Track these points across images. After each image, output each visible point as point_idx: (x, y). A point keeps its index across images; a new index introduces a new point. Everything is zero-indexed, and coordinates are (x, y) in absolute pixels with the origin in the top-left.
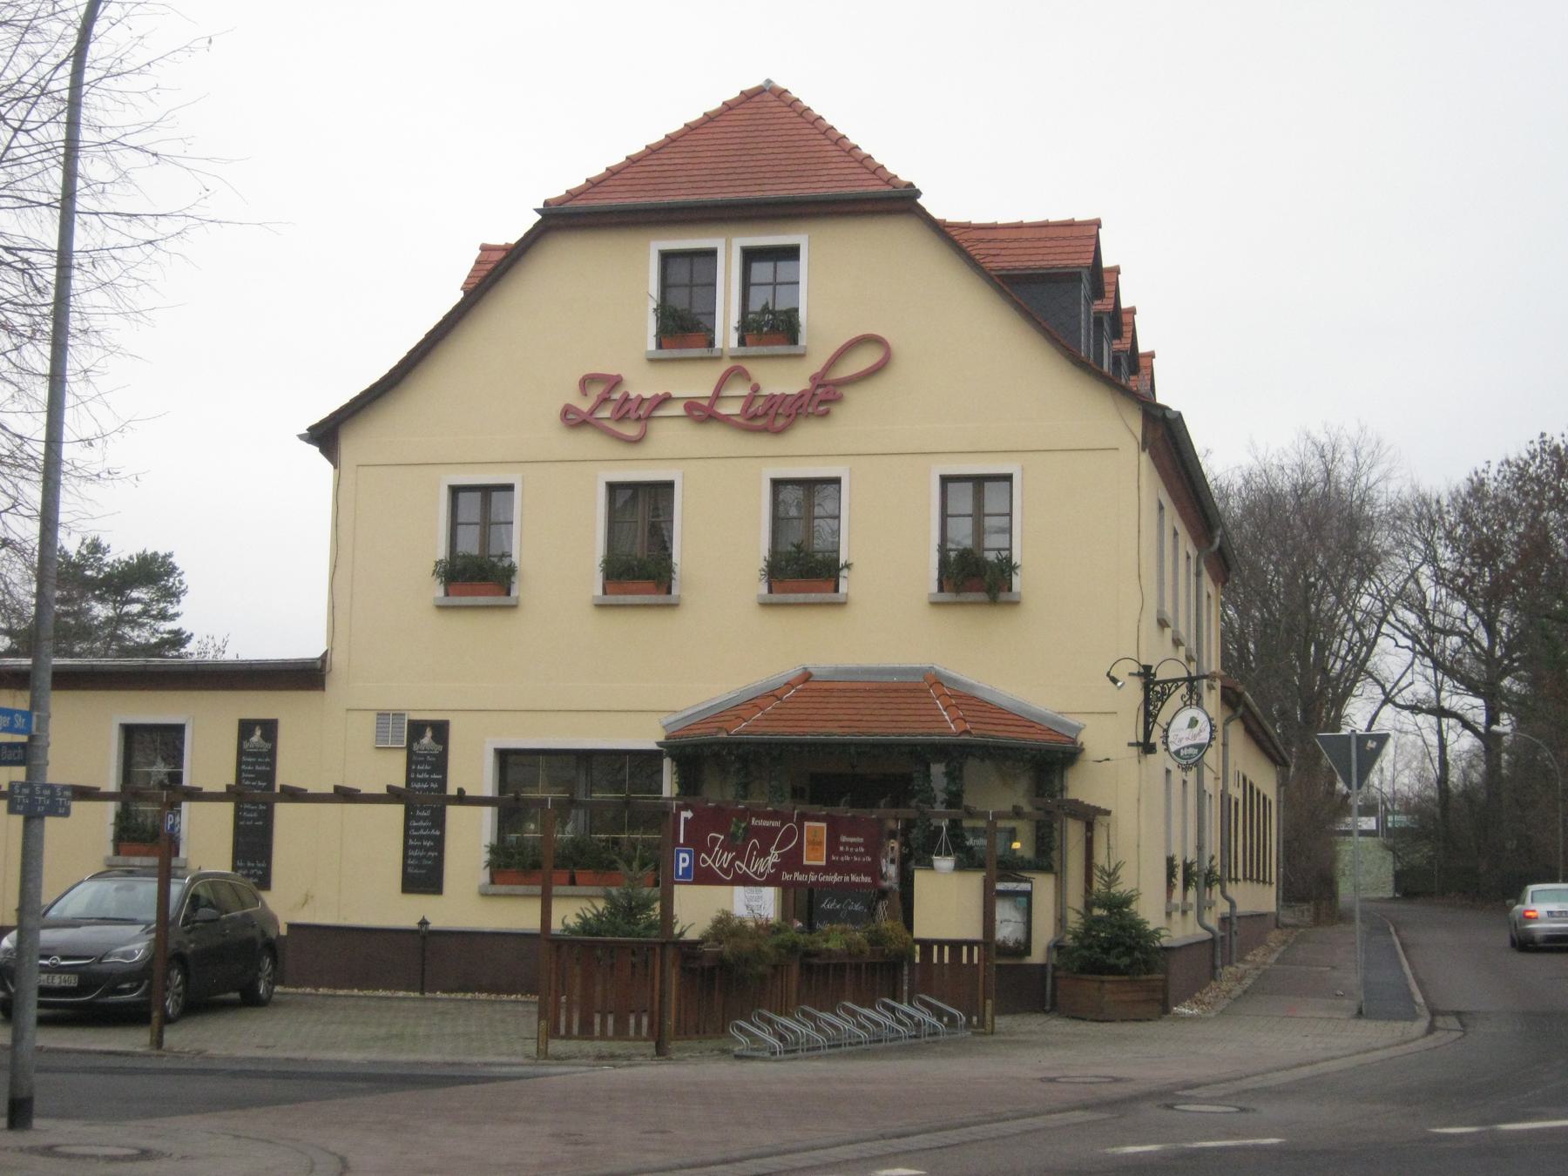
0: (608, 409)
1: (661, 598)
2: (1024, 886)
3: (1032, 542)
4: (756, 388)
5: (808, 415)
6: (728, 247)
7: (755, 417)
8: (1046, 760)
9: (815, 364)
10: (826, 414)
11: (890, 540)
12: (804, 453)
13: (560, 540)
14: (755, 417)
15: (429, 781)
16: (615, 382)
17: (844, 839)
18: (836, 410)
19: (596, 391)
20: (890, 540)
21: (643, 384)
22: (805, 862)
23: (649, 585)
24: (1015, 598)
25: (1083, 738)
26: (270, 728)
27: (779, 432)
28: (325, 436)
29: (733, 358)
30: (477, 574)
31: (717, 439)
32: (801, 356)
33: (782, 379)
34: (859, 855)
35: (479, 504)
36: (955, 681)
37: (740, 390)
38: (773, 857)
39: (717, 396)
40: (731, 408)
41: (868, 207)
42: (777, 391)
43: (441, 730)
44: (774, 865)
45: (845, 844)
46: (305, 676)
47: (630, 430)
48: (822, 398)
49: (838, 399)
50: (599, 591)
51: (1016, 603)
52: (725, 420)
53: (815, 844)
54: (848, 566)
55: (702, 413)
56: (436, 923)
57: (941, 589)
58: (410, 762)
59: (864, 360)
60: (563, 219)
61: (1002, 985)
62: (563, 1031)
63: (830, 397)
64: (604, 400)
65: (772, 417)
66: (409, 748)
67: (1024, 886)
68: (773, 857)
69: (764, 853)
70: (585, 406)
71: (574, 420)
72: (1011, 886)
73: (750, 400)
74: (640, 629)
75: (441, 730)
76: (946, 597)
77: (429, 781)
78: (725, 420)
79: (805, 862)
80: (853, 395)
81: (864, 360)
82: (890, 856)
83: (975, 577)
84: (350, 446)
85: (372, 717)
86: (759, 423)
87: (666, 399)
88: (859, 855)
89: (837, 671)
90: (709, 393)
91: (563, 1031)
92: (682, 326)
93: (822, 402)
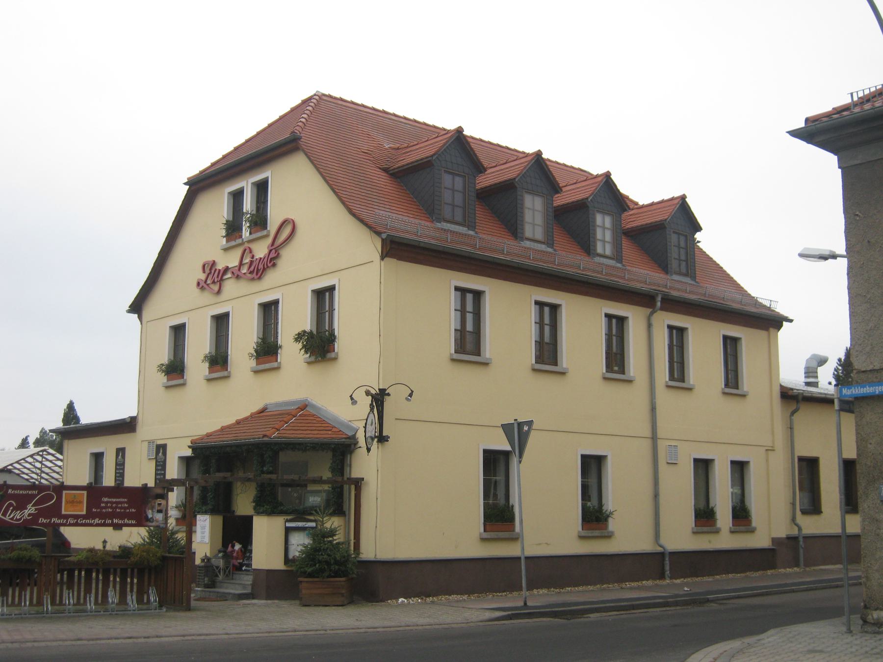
3: (346, 324)
10: (274, 265)
12: (269, 288)
17: (106, 499)
22: (63, 512)
28: (137, 307)
34: (121, 508)
37: (247, 260)
38: (31, 509)
40: (244, 270)
44: (29, 515)
45: (107, 503)
46: (127, 426)
47: (216, 288)
50: (207, 373)
53: (72, 502)
58: (156, 465)
60: (200, 185)
66: (156, 458)
68: (31, 509)
69: (21, 507)
72: (300, 524)
73: (251, 263)
79: (63, 512)
82: (157, 507)
83: (320, 345)
84: (146, 313)
87: (227, 269)
88: (125, 508)
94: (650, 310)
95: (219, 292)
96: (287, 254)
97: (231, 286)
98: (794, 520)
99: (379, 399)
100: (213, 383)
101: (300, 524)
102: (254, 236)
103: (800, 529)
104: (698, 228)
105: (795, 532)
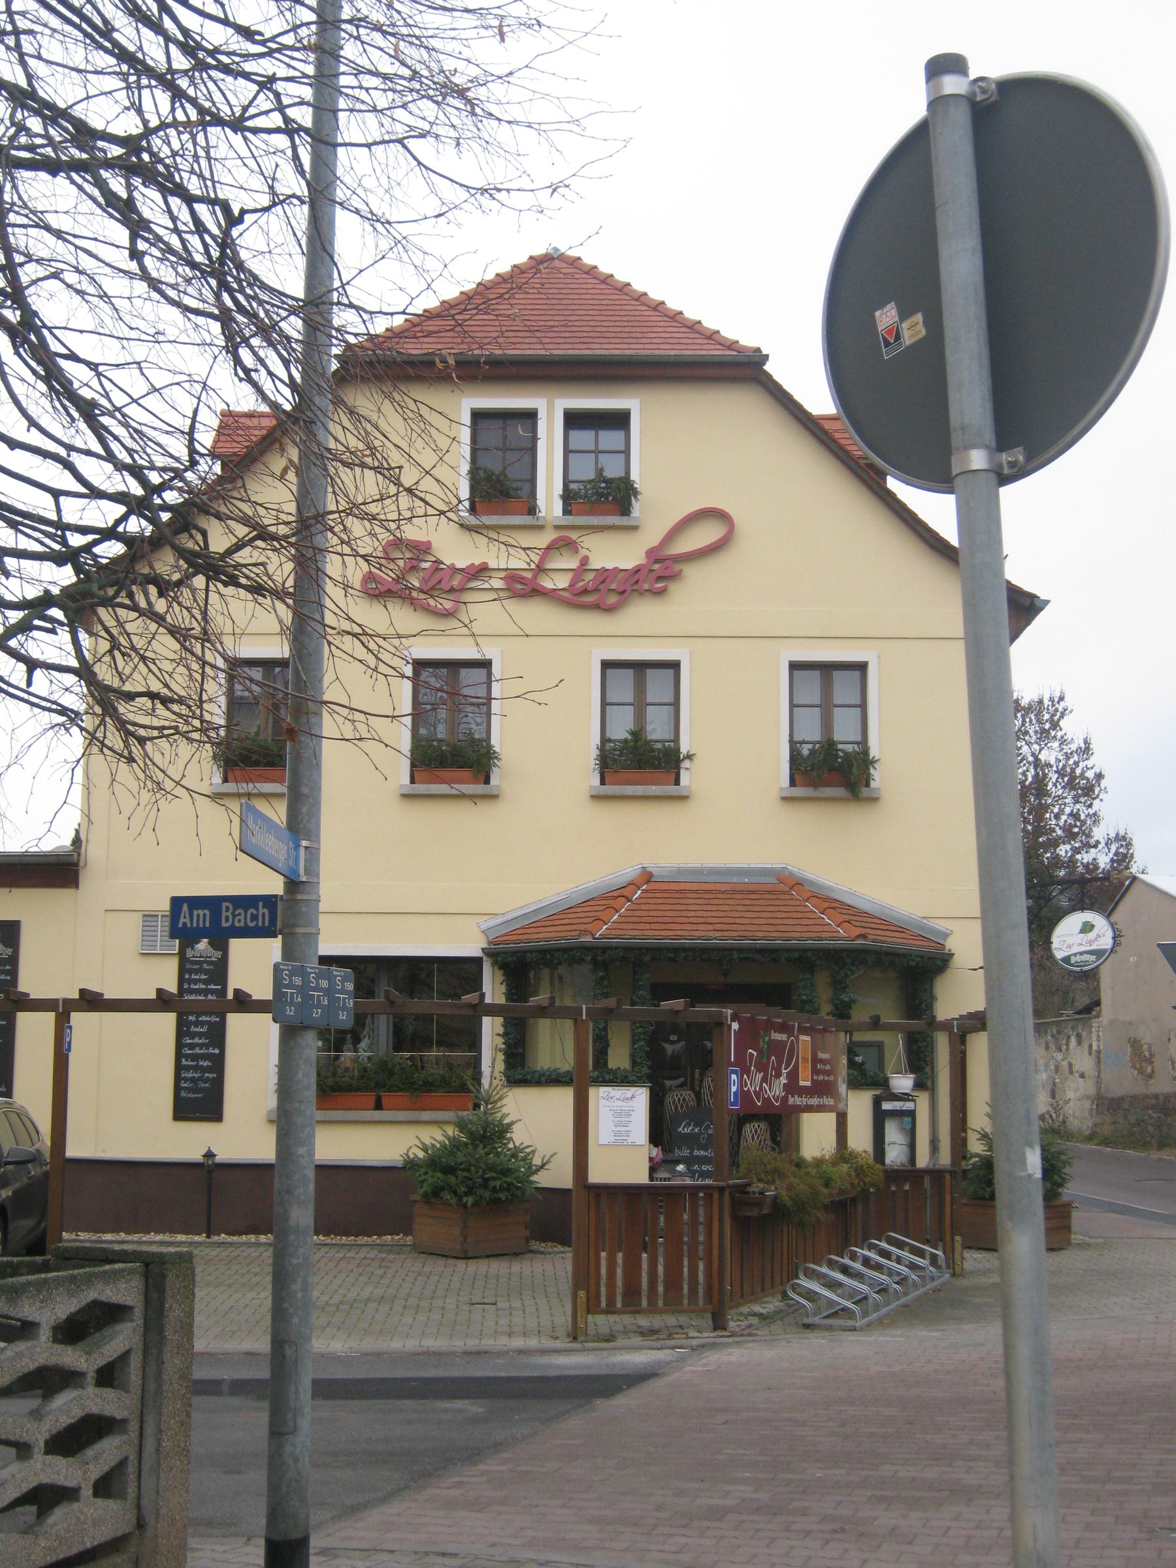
1: (479, 789)
4: (585, 561)
5: (642, 593)
6: (550, 408)
7: (585, 591)
8: (915, 968)
9: (651, 536)
10: (661, 593)
12: (639, 631)
14: (585, 591)
15: (205, 992)
18: (674, 587)
20: (737, 734)
23: (465, 773)
24: (874, 795)
25: (951, 944)
27: (610, 609)
29: (557, 527)
31: (537, 616)
33: (614, 553)
36: (812, 883)
39: (540, 569)
41: (710, 372)
42: (610, 566)
46: (56, 871)
48: (659, 574)
49: (674, 577)
50: (406, 780)
51: (876, 799)
52: (550, 595)
54: (689, 757)
55: (524, 587)
56: (223, 1155)
57: (793, 783)
58: (182, 970)
59: (704, 535)
62: (603, 1304)
63: (667, 573)
65: (599, 594)
74: (453, 822)
76: (799, 791)
77: (205, 992)
78: (550, 595)
80: (693, 573)
81: (704, 535)
85: (138, 917)
86: (589, 599)
87: (481, 571)
89: (680, 871)
91: (603, 1304)
92: (498, 489)
93: (660, 578)
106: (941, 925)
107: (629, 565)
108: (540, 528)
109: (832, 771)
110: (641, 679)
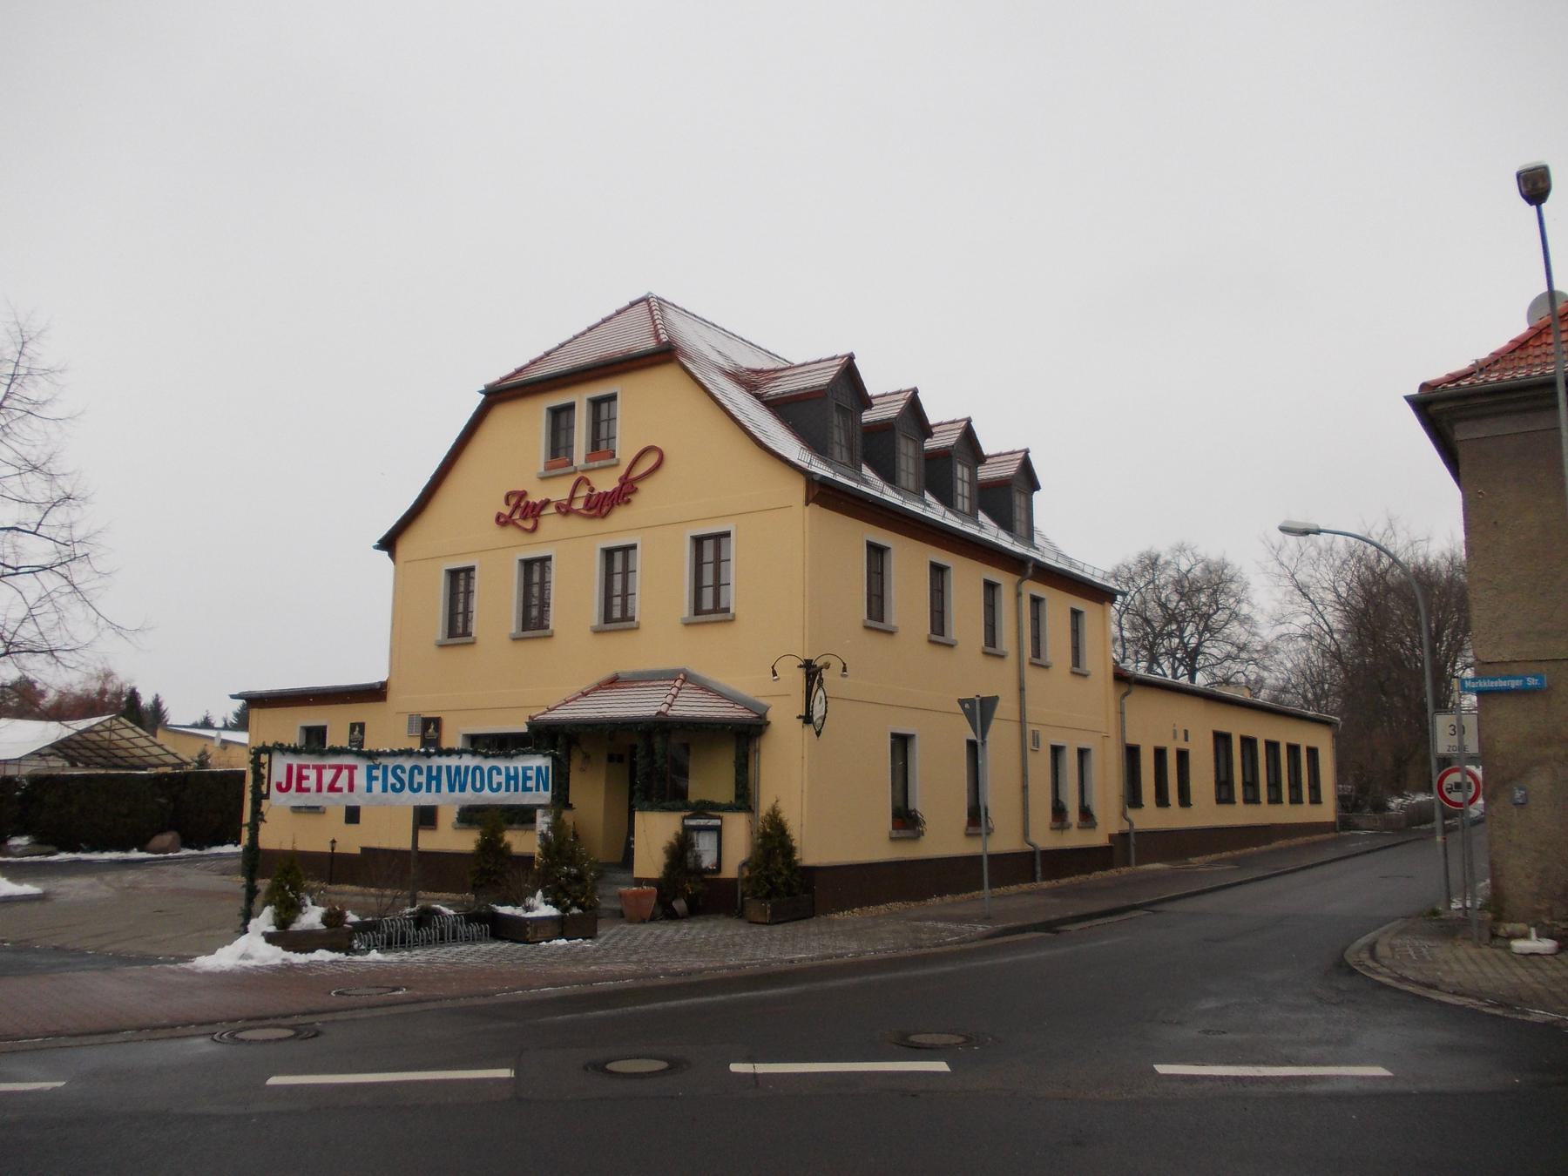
0: (523, 511)
2: (718, 822)
4: (592, 490)
6: (580, 398)
9: (622, 471)
10: (629, 501)
11: (662, 583)
12: (618, 528)
13: (497, 602)
16: (523, 494)
19: (513, 501)
20: (662, 583)
21: (535, 497)
26: (362, 726)
27: (604, 516)
28: (389, 543)
30: (458, 627)
31: (576, 525)
32: (617, 465)
33: (606, 482)
35: (460, 580)
37: (583, 492)
39: (572, 498)
40: (579, 505)
43: (437, 722)
46: (374, 694)
47: (529, 524)
48: (625, 493)
49: (634, 491)
55: (565, 509)
59: (649, 462)
60: (498, 395)
61: (688, 891)
64: (517, 506)
65: (601, 506)
67: (718, 822)
70: (507, 511)
71: (503, 521)
72: (702, 822)
73: (589, 498)
75: (437, 722)
78: (577, 512)
80: (643, 487)
81: (649, 462)
83: (708, 604)
84: (403, 546)
87: (546, 503)
90: (566, 496)
94: (1018, 578)
95: (534, 529)
96: (647, 492)
97: (551, 523)
98: (1124, 814)
99: (812, 672)
100: (519, 643)
101: (702, 822)
102: (591, 465)
103: (1131, 824)
104: (1035, 486)
105: (1126, 827)
106: (764, 701)
107: (609, 489)
108: (575, 472)
109: (708, 604)
110: (617, 560)
